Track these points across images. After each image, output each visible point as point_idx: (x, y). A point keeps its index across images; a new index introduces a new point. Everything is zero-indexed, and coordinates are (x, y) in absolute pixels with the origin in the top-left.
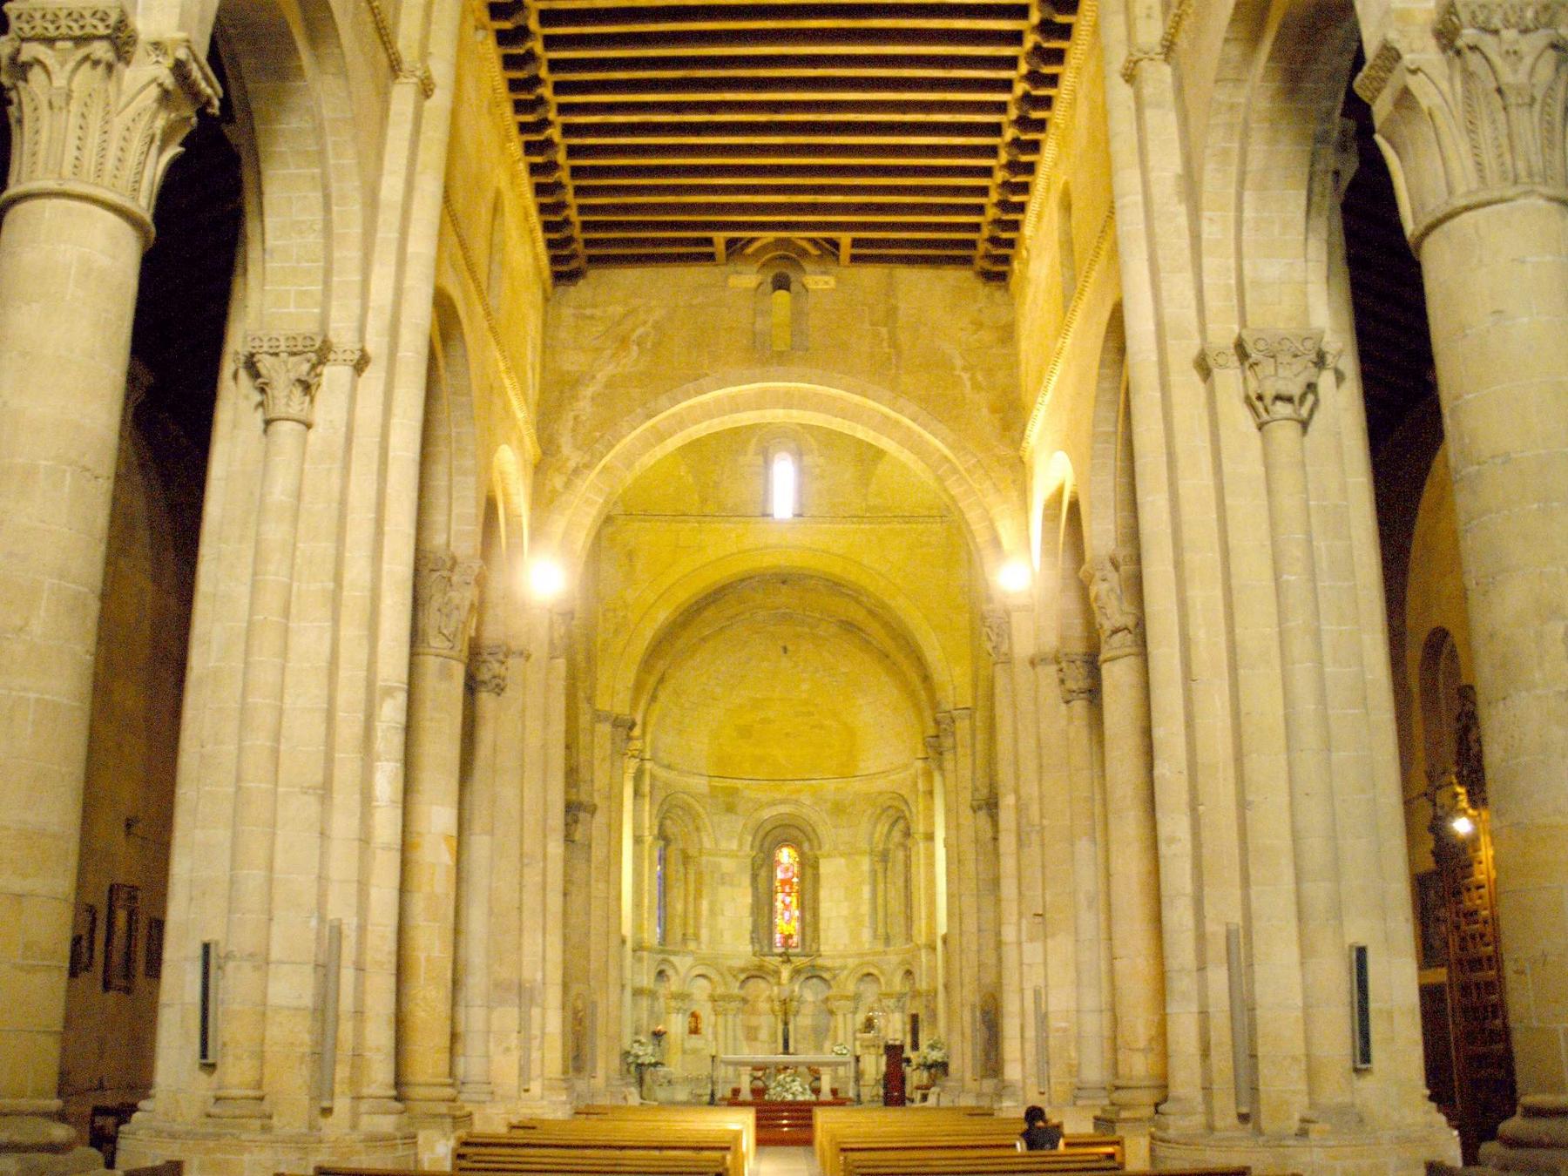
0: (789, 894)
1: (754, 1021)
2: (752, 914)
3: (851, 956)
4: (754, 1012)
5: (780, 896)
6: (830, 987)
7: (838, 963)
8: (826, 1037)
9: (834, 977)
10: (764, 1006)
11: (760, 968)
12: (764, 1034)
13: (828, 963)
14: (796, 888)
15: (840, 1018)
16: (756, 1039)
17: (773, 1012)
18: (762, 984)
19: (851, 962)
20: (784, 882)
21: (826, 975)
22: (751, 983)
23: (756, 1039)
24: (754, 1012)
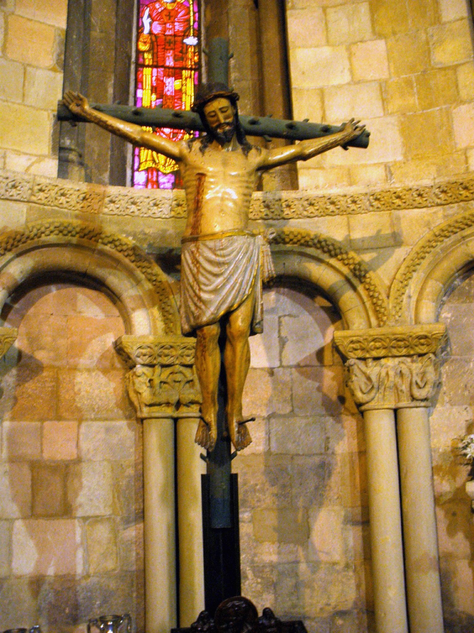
0: (176, 73)
1: (59, 442)
2: (65, 66)
3: (420, 198)
4: (59, 408)
5: (148, 75)
6: (335, 313)
7: (365, 226)
8: (318, 497)
9: (358, 275)
10: (95, 387)
11: (88, 238)
12: (94, 492)
13: (333, 230)
14: (192, 58)
15: (381, 426)
16: (66, 511)
17: (130, 408)
18: (89, 307)
19: (417, 224)
20: (158, 44)
21: (324, 274)
22: (52, 297)
23: (66, 511)
24: (59, 408)
